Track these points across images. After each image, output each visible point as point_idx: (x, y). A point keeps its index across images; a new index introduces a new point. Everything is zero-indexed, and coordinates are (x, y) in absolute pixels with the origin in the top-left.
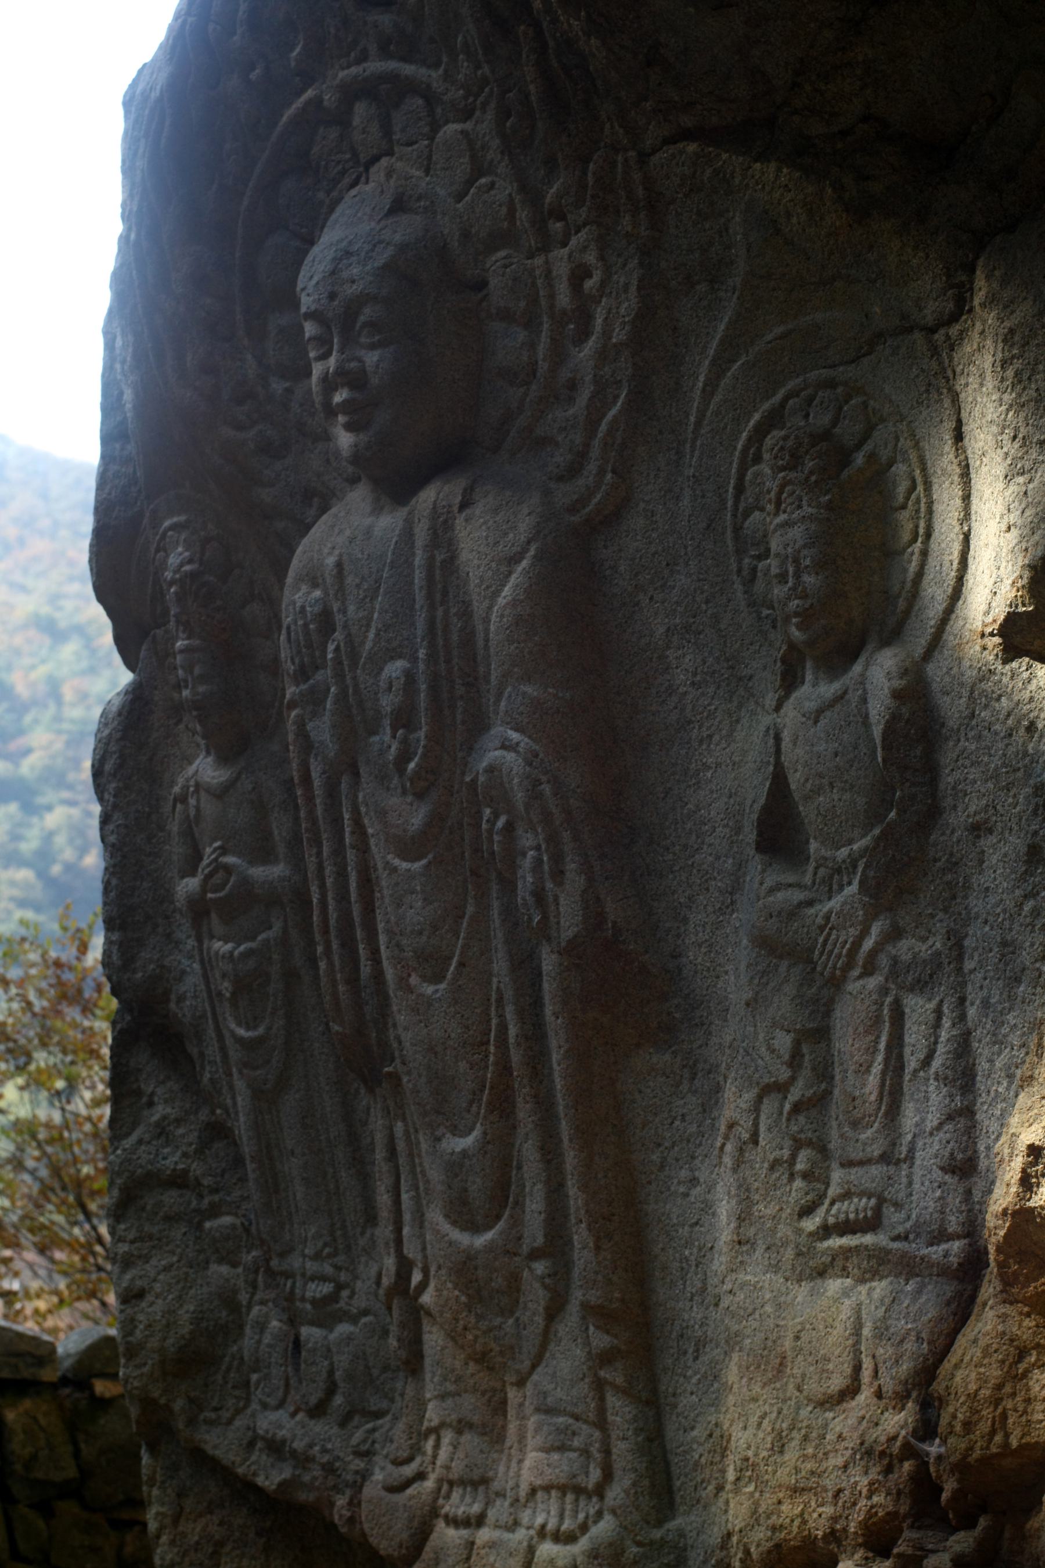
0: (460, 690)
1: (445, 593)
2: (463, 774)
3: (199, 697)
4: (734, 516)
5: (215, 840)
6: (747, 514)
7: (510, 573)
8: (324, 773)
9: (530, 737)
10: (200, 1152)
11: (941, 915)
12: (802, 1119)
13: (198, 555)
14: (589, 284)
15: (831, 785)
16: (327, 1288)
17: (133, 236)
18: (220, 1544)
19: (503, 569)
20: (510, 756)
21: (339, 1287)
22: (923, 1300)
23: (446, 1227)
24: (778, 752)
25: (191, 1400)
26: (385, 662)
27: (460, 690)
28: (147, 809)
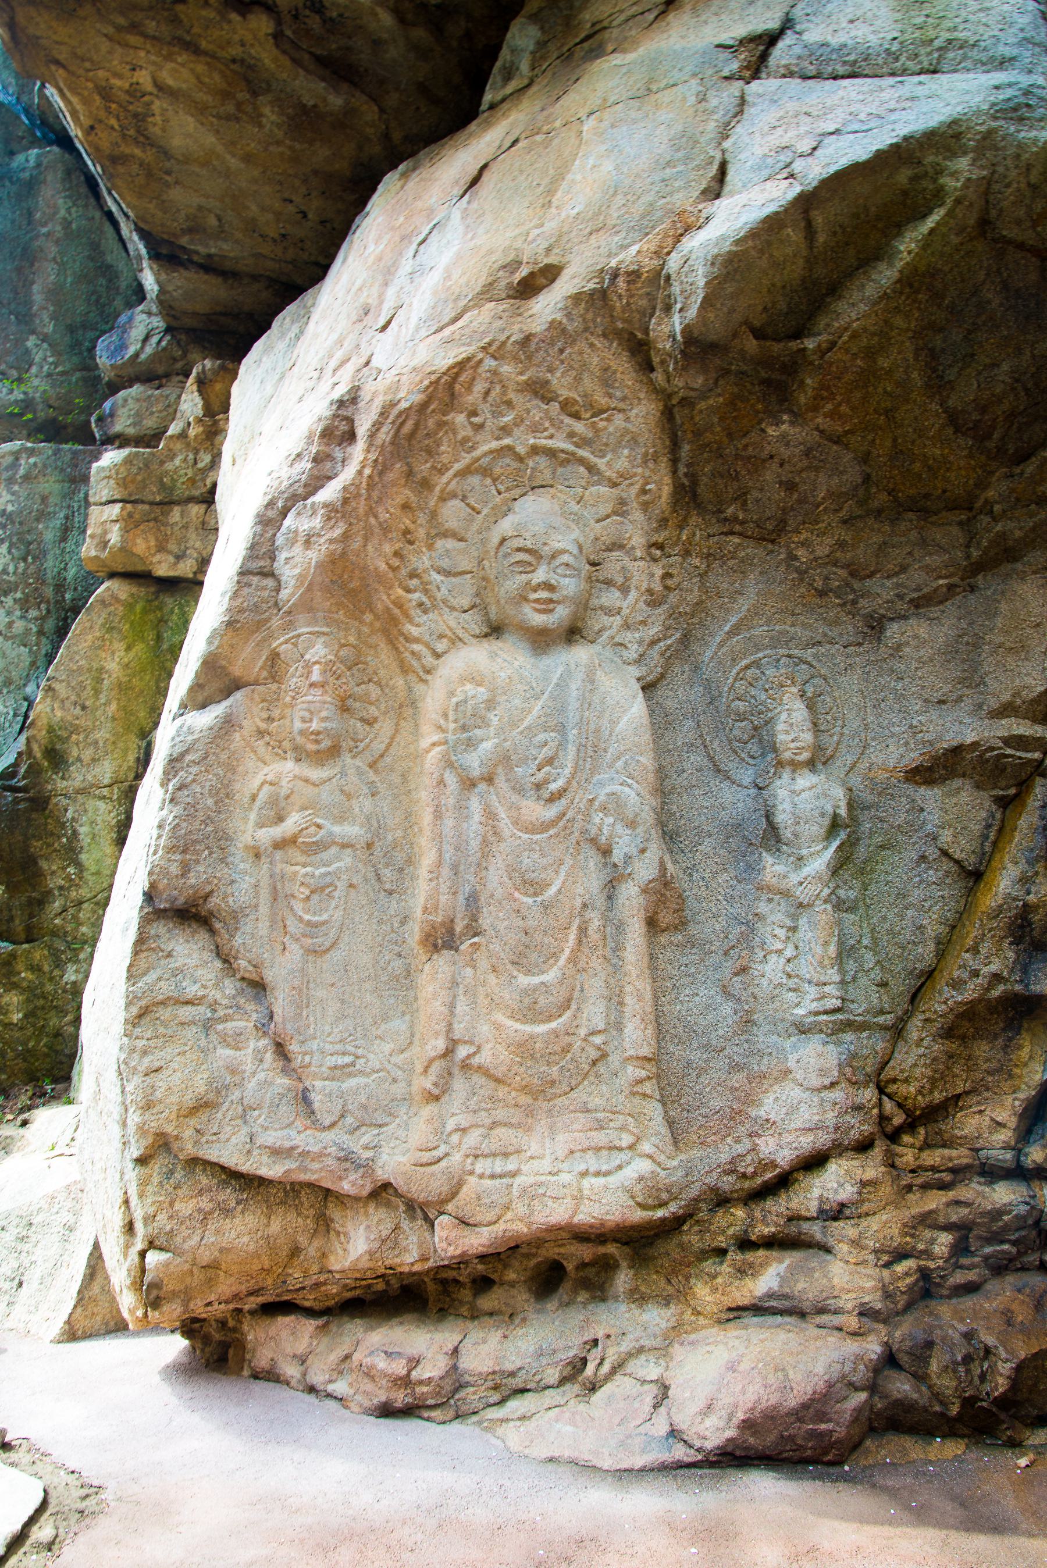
17: (367, 471)
20: (627, 789)
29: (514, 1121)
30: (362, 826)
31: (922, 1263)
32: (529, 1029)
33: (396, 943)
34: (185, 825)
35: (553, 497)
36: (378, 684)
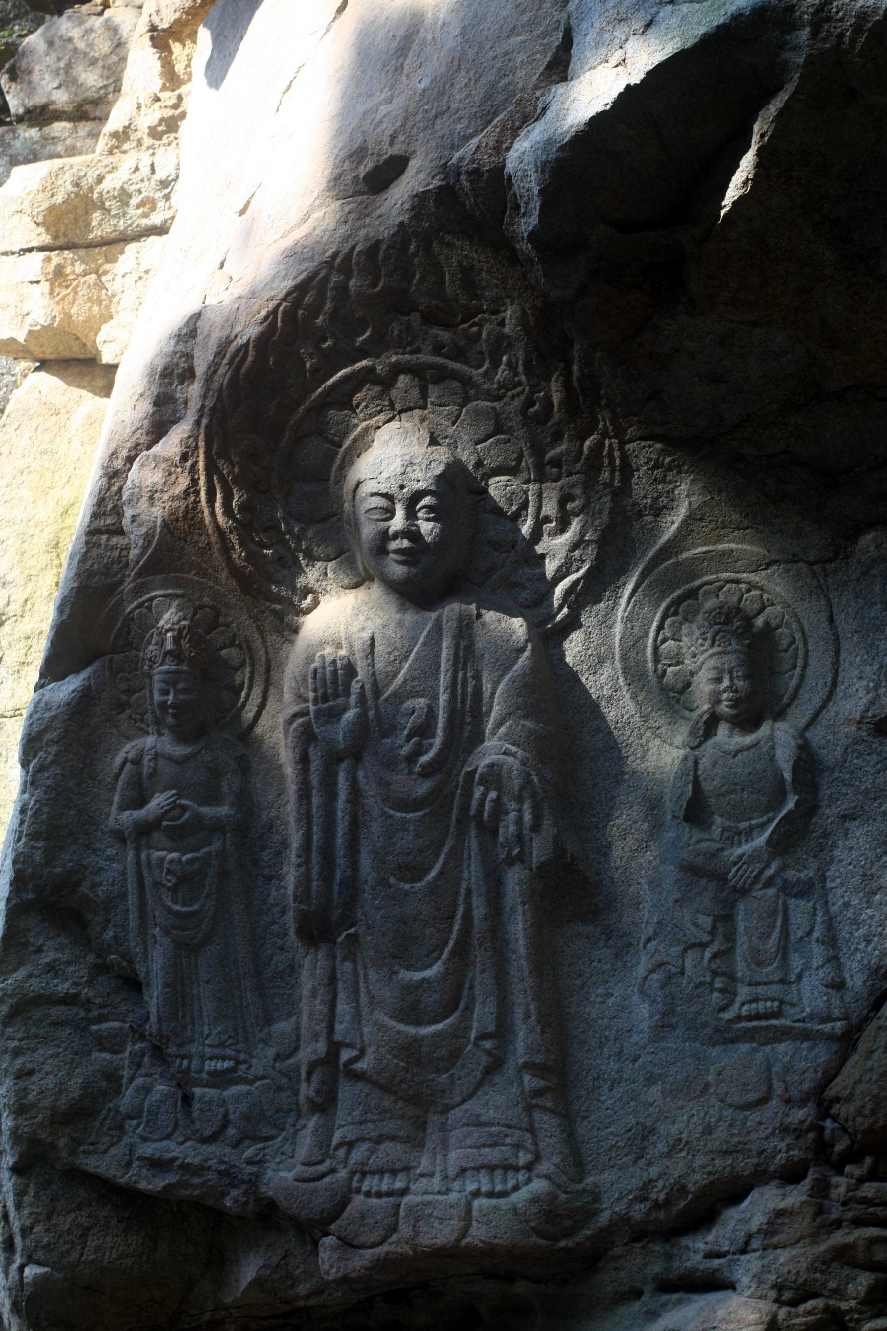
0: (468, 719)
1: (465, 665)
2: (463, 766)
4: (655, 640)
5: (170, 789)
6: (664, 641)
7: (518, 658)
9: (524, 750)
10: (89, 983)
11: (811, 859)
12: (718, 961)
14: (569, 506)
15: (743, 790)
16: (232, 1063)
18: (89, 1229)
19: (513, 655)
20: (510, 759)
21: (238, 1063)
22: (816, 1051)
23: (392, 1023)
24: (696, 769)
25: (73, 1139)
26: (408, 698)
27: (468, 719)
29: (401, 1134)
31: (831, 1303)
32: (411, 1030)
33: (278, 936)
34: (46, 809)
35: (422, 420)
36: (240, 646)
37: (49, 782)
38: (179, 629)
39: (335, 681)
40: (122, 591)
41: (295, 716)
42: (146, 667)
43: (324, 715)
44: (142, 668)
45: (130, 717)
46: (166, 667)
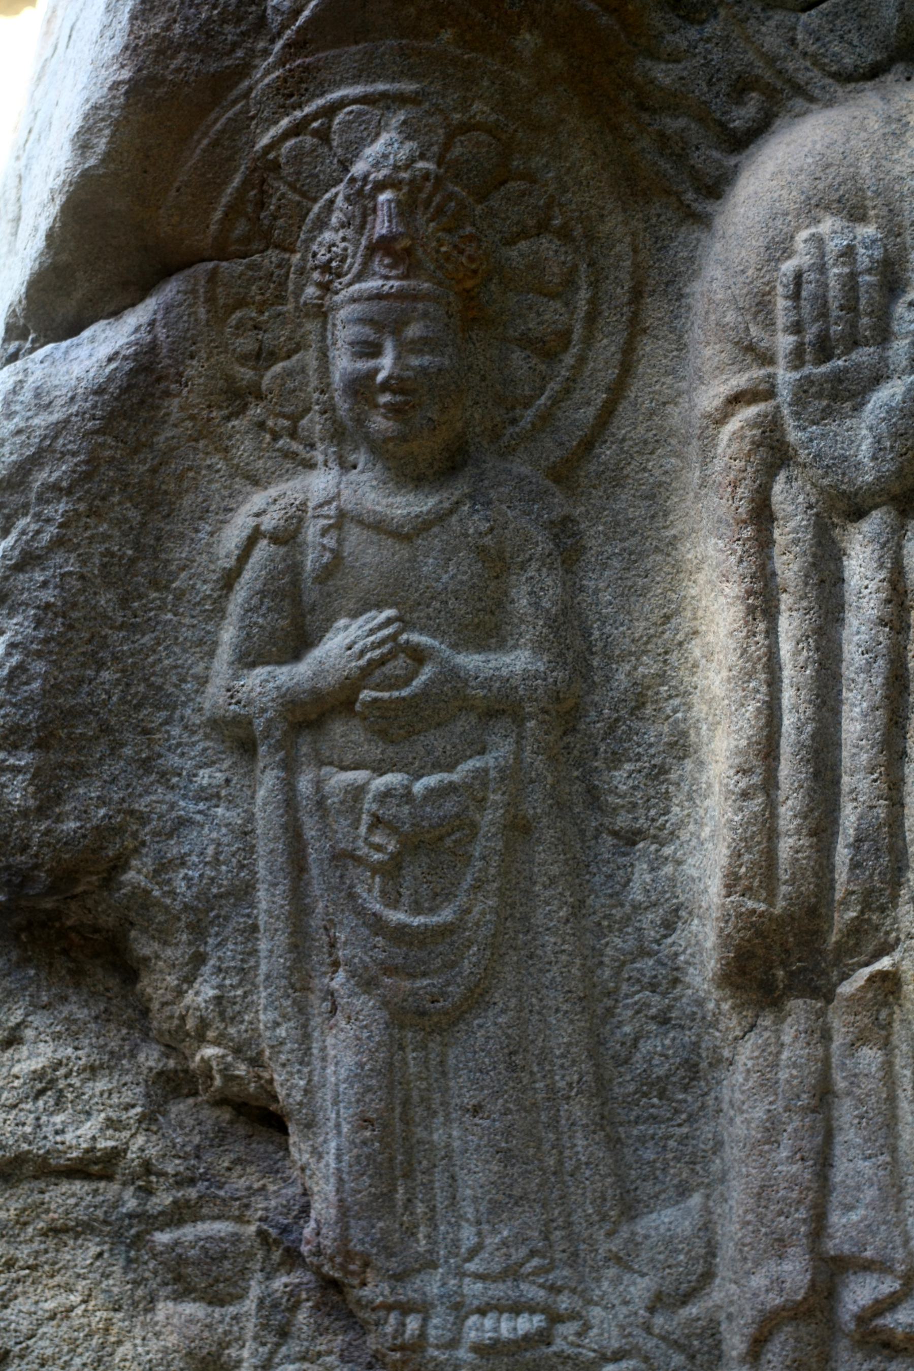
3: (410, 373)
5: (379, 606)
8: (810, 507)
10: (148, 1120)
13: (435, 149)
16: (538, 1321)
21: (555, 1318)
28: (130, 552)
30: (539, 647)
33: (653, 987)
34: (39, 667)
36: (564, 234)
37: (48, 596)
38: (412, 181)
39: (851, 306)
40: (246, 95)
41: (737, 400)
42: (311, 291)
43: (819, 395)
44: (300, 289)
45: (261, 425)
46: (372, 284)
